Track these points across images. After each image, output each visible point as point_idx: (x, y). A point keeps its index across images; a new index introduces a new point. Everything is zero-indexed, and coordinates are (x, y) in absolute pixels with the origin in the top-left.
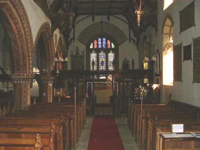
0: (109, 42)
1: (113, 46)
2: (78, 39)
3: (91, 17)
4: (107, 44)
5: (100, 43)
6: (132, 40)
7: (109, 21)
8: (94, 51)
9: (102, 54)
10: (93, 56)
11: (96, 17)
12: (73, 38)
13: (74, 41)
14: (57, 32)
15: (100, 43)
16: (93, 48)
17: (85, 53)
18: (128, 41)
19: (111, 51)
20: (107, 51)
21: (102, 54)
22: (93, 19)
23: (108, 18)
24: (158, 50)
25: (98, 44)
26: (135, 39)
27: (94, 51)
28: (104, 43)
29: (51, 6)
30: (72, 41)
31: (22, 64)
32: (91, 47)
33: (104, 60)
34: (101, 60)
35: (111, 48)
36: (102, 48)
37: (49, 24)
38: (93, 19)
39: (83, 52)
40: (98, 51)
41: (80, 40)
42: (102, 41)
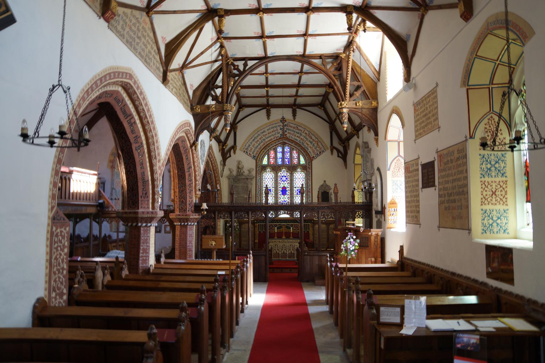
0: (295, 155)
1: (302, 161)
2: (240, 150)
3: (264, 111)
5: (279, 155)
6: (335, 152)
7: (294, 118)
9: (283, 173)
10: (268, 179)
11: (273, 111)
12: (234, 147)
13: (235, 152)
14: (205, 136)
15: (279, 155)
16: (269, 165)
18: (329, 151)
19: (299, 170)
20: (292, 169)
21: (283, 173)
22: (268, 115)
23: (294, 114)
24: (378, 169)
25: (276, 158)
26: (341, 148)
28: (288, 155)
29: (195, 92)
30: (232, 151)
31: (140, 194)
32: (265, 162)
33: (286, 186)
34: (282, 186)
36: (283, 165)
37: (190, 125)
38: (268, 115)
39: (250, 171)
40: (276, 169)
42: (283, 152)
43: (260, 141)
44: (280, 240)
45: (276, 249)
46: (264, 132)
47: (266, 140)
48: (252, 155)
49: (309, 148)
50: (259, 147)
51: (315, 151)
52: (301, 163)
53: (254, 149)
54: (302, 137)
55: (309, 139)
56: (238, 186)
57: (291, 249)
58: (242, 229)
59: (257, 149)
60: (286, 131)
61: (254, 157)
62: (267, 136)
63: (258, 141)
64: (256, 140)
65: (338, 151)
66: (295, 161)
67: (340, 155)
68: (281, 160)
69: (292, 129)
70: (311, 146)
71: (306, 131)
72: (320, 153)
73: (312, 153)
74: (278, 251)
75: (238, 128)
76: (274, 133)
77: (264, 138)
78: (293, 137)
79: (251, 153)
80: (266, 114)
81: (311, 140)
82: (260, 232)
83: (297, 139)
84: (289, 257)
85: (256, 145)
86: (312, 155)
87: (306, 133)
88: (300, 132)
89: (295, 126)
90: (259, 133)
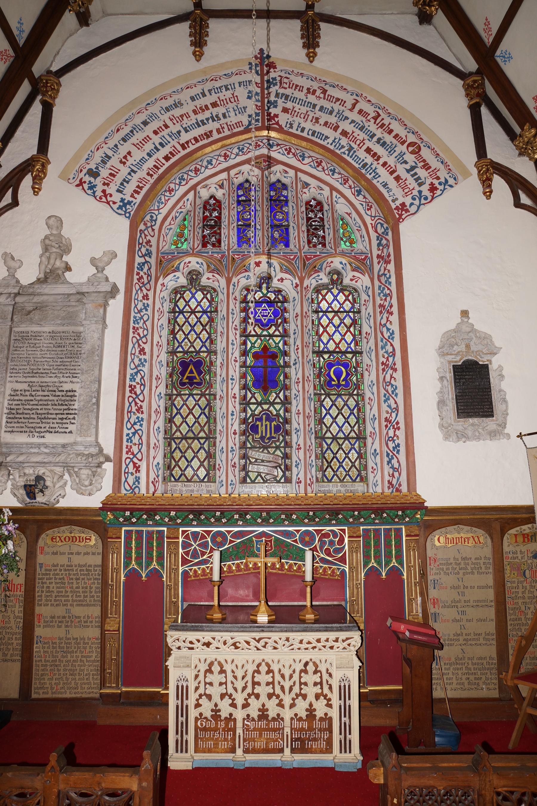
17: (117, 273)
18: (473, 183)
23: (311, 41)
41: (88, 179)
43: (156, 139)
44: (241, 637)
45: (215, 691)
46: (178, 104)
47: (185, 137)
48: (117, 197)
49: (381, 171)
50: (151, 163)
51: (411, 183)
53: (124, 171)
54: (345, 126)
55: (379, 133)
56: (37, 335)
57: (311, 691)
58: (41, 558)
59: (142, 174)
60: (275, 104)
61: (124, 204)
62: (186, 122)
63: (147, 139)
64: (139, 136)
65: (516, 182)
67: (525, 199)
69: (300, 95)
70: (391, 161)
71: (362, 105)
72: (433, 189)
73: (398, 192)
74: (225, 710)
75: (63, 92)
76: (220, 110)
77: (174, 128)
78: (308, 125)
79: (112, 189)
80: (188, 40)
81: (388, 139)
82: (132, 576)
83: (327, 131)
84: (301, 746)
85: (138, 155)
86: (396, 195)
87: (360, 112)
88: (337, 107)
89: (315, 85)
90: (155, 109)
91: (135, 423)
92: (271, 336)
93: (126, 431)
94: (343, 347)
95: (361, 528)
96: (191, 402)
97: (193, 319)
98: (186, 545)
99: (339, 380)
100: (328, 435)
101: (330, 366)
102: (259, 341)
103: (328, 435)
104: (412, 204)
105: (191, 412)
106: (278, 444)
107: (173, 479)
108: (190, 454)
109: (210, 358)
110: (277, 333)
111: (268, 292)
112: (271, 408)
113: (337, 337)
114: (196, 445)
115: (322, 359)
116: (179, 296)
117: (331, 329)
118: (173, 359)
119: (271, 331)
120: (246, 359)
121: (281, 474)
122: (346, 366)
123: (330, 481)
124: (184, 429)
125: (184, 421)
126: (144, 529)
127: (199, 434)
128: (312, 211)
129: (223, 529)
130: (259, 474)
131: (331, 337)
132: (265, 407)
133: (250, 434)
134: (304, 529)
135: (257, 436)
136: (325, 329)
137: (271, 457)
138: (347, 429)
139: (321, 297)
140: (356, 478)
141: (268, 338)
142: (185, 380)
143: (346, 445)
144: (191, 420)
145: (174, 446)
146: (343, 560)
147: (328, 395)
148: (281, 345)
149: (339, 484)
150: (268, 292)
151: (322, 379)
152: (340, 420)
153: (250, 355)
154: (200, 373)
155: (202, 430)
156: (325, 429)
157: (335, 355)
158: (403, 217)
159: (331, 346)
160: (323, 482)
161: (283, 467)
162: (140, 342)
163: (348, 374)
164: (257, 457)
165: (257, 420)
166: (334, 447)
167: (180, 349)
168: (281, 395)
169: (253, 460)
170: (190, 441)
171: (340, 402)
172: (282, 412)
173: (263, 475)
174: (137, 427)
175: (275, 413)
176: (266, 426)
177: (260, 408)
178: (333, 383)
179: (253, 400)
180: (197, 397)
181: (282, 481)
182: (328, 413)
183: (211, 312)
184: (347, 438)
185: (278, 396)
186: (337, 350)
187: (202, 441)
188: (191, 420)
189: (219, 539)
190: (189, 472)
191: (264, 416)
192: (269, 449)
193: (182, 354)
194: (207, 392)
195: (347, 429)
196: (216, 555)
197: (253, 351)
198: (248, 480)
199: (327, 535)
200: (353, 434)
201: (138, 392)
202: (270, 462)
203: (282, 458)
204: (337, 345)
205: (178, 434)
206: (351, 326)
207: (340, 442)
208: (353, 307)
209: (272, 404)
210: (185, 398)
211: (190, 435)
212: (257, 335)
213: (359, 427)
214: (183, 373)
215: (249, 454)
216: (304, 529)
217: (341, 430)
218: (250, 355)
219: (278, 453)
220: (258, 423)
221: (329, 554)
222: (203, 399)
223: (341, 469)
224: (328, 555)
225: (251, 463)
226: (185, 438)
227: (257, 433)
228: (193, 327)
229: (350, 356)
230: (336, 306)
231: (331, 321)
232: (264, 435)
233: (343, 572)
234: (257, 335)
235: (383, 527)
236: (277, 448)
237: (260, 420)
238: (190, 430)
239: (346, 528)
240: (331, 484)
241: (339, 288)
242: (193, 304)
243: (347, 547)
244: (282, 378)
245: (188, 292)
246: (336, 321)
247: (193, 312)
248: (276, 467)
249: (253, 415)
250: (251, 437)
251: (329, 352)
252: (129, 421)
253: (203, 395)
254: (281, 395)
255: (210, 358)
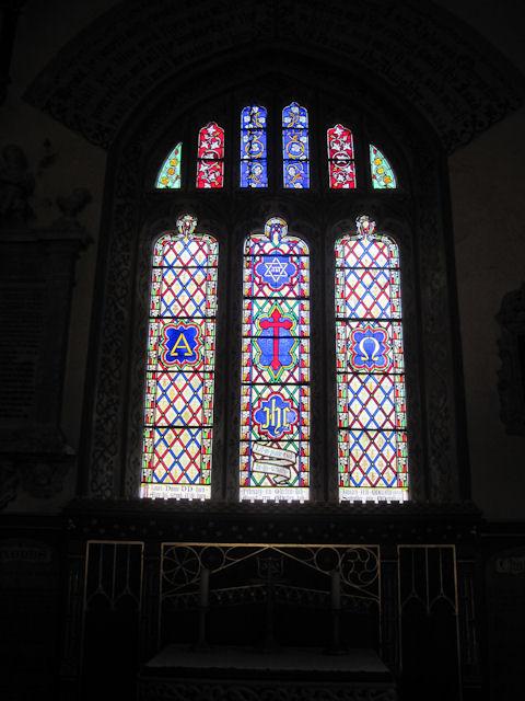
0: (340, 142)
1: (383, 174)
4: (319, 159)
5: (253, 145)
8: (188, 221)
15: (253, 145)
16: (190, 197)
19: (364, 223)
20: (322, 217)
27: (188, 221)
32: (169, 176)
35: (363, 198)
36: (275, 199)
42: (274, 133)
52: (378, 185)
66: (343, 177)
68: (258, 170)
91: (108, 407)
92: (284, 299)
93: (95, 416)
94: (376, 313)
95: (399, 547)
96: (180, 382)
97: (185, 277)
98: (169, 565)
99: (370, 356)
100: (356, 425)
101: (359, 336)
102: (269, 305)
103: (356, 425)
104: (463, 132)
105: (180, 393)
106: (291, 436)
107: (155, 481)
108: (177, 448)
109: (206, 326)
110: (291, 295)
111: (281, 243)
112: (283, 391)
113: (368, 301)
114: (186, 437)
115: (348, 329)
116: (167, 247)
117: (360, 291)
118: (158, 327)
119: (284, 292)
120: (251, 328)
121: (294, 475)
122: (379, 336)
123: (358, 486)
124: (171, 415)
125: (171, 405)
126: (115, 543)
127: (189, 422)
128: (337, 142)
129: (216, 545)
130: (267, 475)
131: (360, 301)
132: (276, 388)
133: (255, 424)
134: (324, 546)
135: (264, 426)
136: (353, 292)
137: (281, 454)
138: (380, 418)
139: (347, 250)
140: (393, 482)
141: (279, 301)
142: (173, 354)
143: (380, 440)
144: (179, 404)
145: (157, 437)
146: (374, 588)
147: (356, 374)
148: (296, 310)
149: (371, 490)
150: (281, 243)
151: (349, 354)
152: (372, 406)
153: (257, 322)
154: (192, 344)
155: (194, 416)
156: (352, 418)
157: (366, 323)
158: (453, 148)
159: (361, 312)
160: (349, 486)
161: (297, 466)
162: (117, 304)
163: (382, 348)
164: (263, 453)
165: (265, 405)
166: (364, 441)
167: (168, 314)
168: (296, 374)
169: (258, 457)
170: (178, 431)
171: (371, 384)
172: (296, 396)
173: (271, 477)
174: (111, 412)
175: (287, 396)
176: (276, 412)
177: (268, 391)
178: (363, 359)
179: (260, 380)
180: (188, 375)
181: (296, 484)
182: (356, 397)
183: (208, 267)
184: (380, 430)
185: (291, 375)
186: (369, 317)
187: (194, 431)
188: (179, 404)
189: (212, 557)
190: (176, 472)
191: (274, 401)
192: (280, 443)
193: (170, 320)
194: (202, 369)
195: (380, 418)
196: (206, 575)
197: (260, 317)
198: (252, 483)
199: (353, 555)
200: (388, 426)
201: (114, 367)
202: (278, 459)
203: (296, 455)
204: (369, 310)
205: (163, 423)
206: (386, 286)
207: (372, 434)
208: (389, 262)
209: (283, 385)
210: (173, 375)
211: (179, 423)
212: (266, 298)
213: (396, 416)
214: (171, 345)
215: (254, 450)
216: (324, 546)
217: (372, 419)
218: (257, 322)
219: (291, 448)
220: (266, 409)
221: (355, 581)
222: (196, 377)
223: (373, 470)
224: (354, 582)
225: (255, 460)
226: (171, 427)
227: (265, 423)
228: (184, 287)
229: (384, 324)
230: (367, 261)
231: (360, 280)
232: (273, 424)
233: (375, 603)
234: (266, 298)
235: (427, 546)
236: (291, 441)
237: (269, 405)
238: (179, 417)
239: (379, 547)
240: (359, 490)
241: (372, 238)
242: (185, 257)
243: (379, 571)
244: (297, 352)
245: (179, 242)
246: (367, 280)
247: (185, 268)
248: (287, 467)
249: (259, 399)
250: (256, 427)
251: (357, 319)
252: (99, 403)
253: (196, 372)
254: (296, 374)
255: (206, 326)
